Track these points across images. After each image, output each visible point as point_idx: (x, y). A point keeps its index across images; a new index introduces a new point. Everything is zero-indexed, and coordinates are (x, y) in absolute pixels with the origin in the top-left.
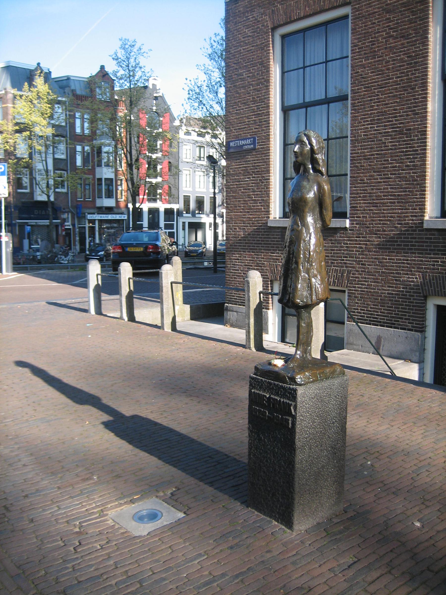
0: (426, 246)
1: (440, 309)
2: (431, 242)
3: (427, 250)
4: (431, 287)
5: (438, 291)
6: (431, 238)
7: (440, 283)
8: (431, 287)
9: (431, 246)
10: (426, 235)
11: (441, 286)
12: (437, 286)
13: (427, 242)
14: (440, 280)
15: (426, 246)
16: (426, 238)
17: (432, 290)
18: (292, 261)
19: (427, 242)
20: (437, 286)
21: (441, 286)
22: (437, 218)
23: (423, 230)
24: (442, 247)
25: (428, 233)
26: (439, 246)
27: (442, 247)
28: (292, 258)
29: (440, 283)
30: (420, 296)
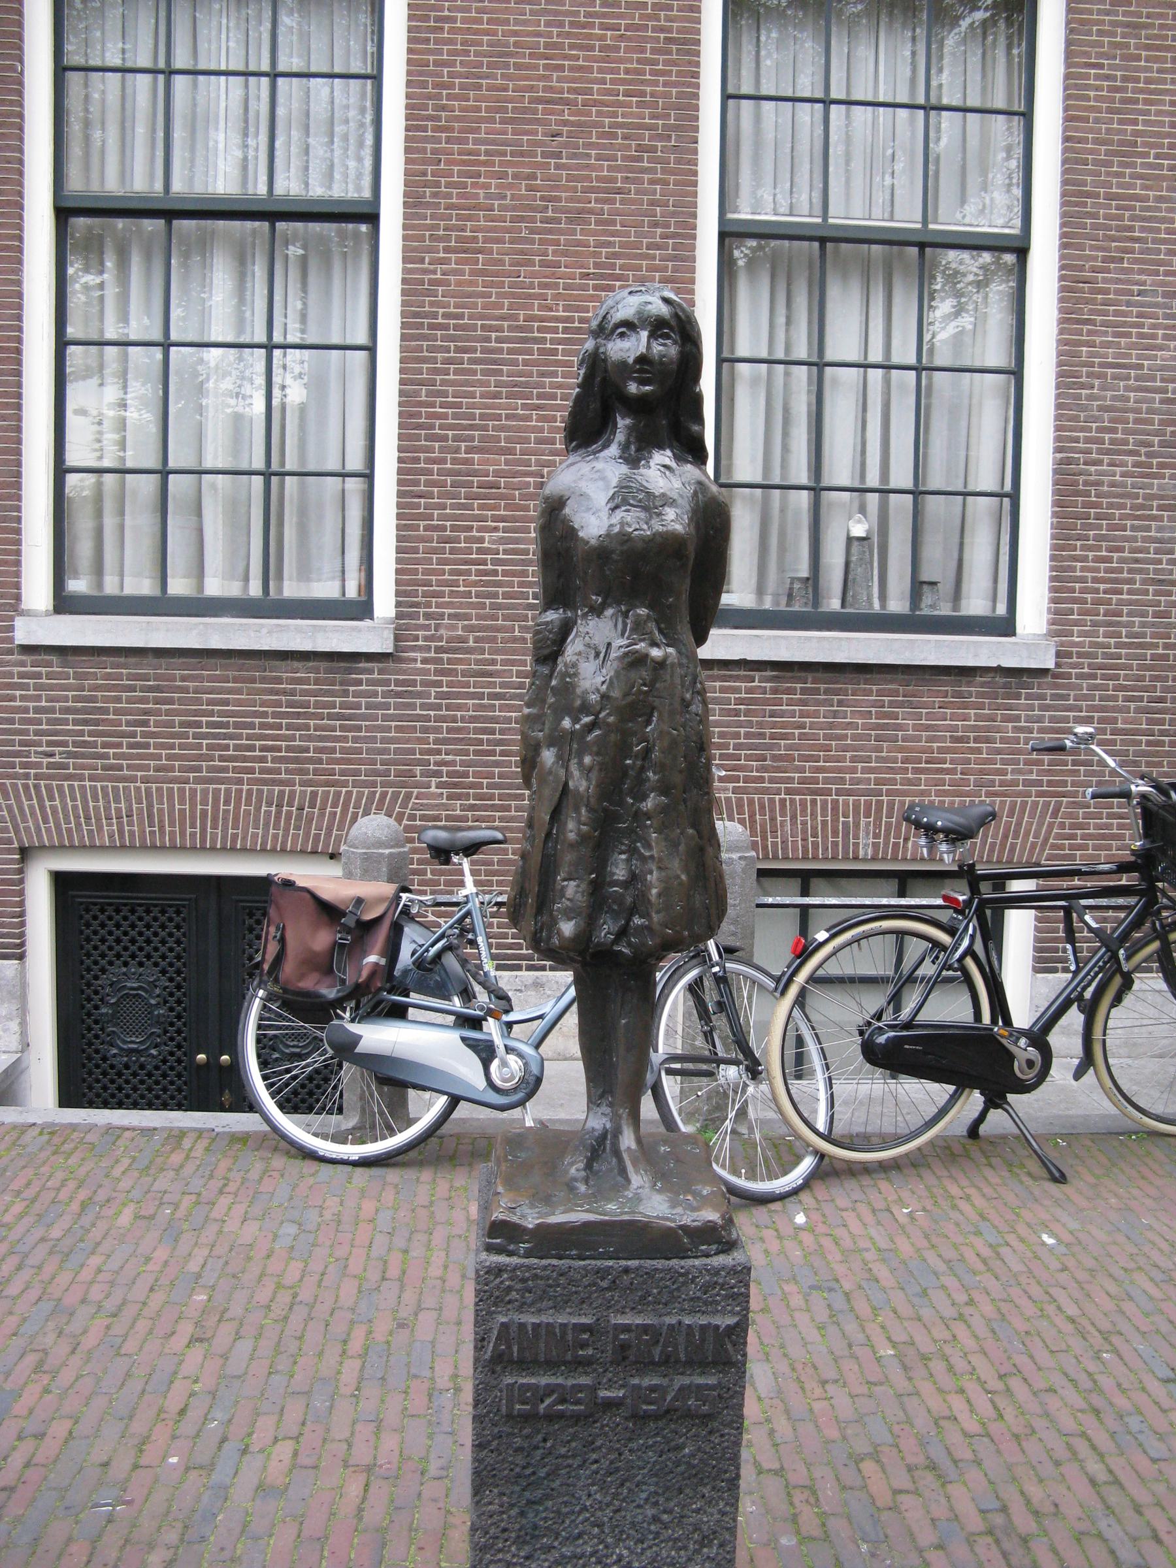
0: (23, 698)
1: (62, 882)
2: (37, 687)
3: (26, 710)
4: (46, 821)
5: (69, 830)
6: (38, 676)
7: (75, 807)
8: (46, 821)
9: (38, 698)
10: (23, 664)
11: (77, 817)
12: (66, 816)
13: (24, 687)
14: (74, 799)
15: (23, 698)
16: (22, 675)
17: (48, 830)
18: (640, 780)
19: (24, 687)
20: (66, 816)
21: (77, 817)
22: (47, 614)
23: (10, 652)
24: (76, 699)
25: (28, 659)
26: (66, 699)
27: (76, 699)
28: (643, 769)
29: (75, 807)
30: (9, 851)
